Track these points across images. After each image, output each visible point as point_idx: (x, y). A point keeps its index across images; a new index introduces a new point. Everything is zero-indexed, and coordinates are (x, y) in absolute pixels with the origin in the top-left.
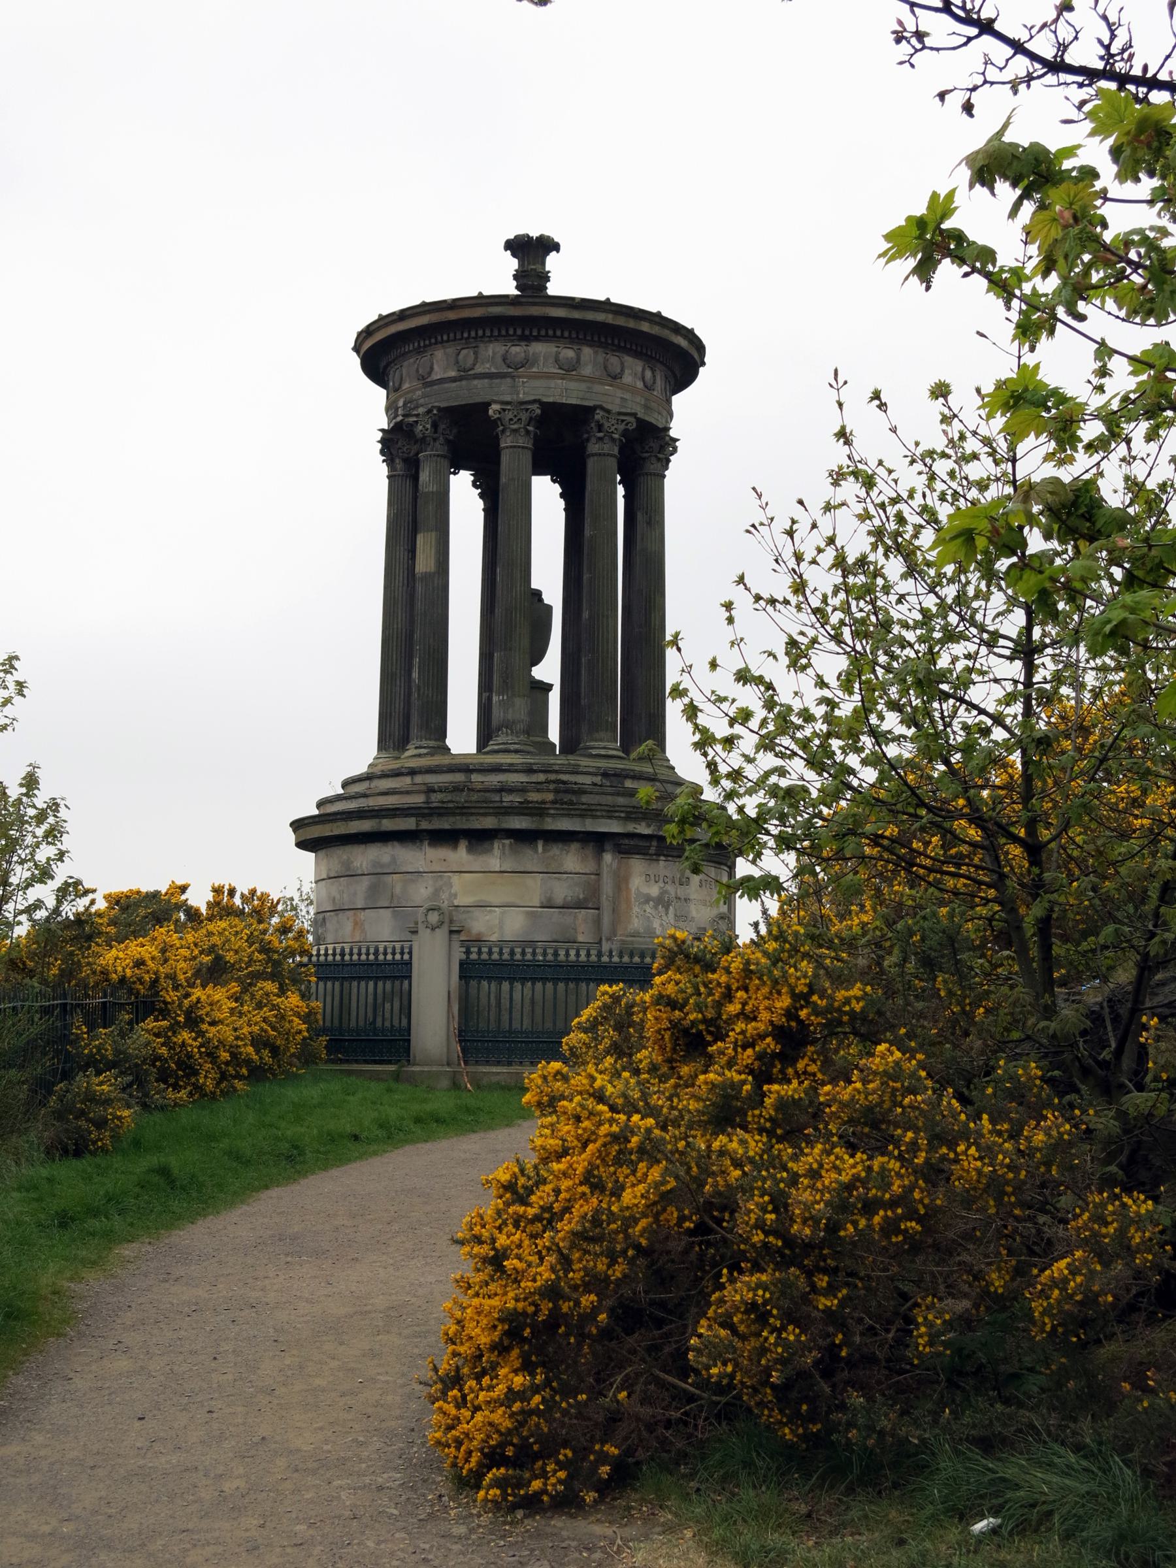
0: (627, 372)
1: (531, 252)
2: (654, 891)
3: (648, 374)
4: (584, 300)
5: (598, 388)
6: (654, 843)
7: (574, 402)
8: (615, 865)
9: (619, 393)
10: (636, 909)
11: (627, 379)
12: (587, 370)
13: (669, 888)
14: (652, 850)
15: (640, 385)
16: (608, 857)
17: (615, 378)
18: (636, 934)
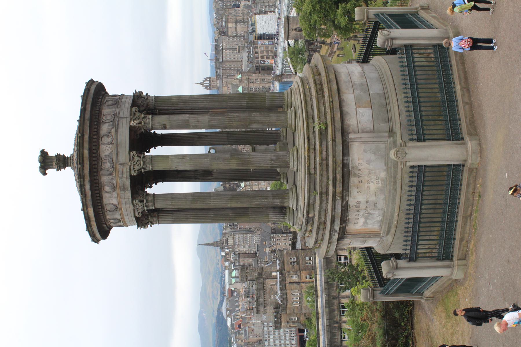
0: (111, 202)
1: (47, 162)
2: (362, 220)
3: (107, 188)
4: (91, 236)
5: (125, 213)
6: (342, 226)
7: (134, 219)
8: (350, 236)
9: (123, 206)
10: (370, 226)
11: (115, 202)
12: (119, 217)
13: (361, 214)
14: (344, 225)
15: (115, 194)
16: (346, 239)
17: (117, 208)
18: (381, 227)
